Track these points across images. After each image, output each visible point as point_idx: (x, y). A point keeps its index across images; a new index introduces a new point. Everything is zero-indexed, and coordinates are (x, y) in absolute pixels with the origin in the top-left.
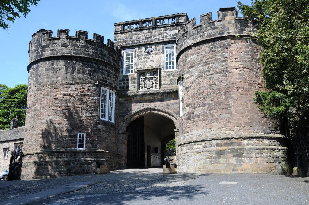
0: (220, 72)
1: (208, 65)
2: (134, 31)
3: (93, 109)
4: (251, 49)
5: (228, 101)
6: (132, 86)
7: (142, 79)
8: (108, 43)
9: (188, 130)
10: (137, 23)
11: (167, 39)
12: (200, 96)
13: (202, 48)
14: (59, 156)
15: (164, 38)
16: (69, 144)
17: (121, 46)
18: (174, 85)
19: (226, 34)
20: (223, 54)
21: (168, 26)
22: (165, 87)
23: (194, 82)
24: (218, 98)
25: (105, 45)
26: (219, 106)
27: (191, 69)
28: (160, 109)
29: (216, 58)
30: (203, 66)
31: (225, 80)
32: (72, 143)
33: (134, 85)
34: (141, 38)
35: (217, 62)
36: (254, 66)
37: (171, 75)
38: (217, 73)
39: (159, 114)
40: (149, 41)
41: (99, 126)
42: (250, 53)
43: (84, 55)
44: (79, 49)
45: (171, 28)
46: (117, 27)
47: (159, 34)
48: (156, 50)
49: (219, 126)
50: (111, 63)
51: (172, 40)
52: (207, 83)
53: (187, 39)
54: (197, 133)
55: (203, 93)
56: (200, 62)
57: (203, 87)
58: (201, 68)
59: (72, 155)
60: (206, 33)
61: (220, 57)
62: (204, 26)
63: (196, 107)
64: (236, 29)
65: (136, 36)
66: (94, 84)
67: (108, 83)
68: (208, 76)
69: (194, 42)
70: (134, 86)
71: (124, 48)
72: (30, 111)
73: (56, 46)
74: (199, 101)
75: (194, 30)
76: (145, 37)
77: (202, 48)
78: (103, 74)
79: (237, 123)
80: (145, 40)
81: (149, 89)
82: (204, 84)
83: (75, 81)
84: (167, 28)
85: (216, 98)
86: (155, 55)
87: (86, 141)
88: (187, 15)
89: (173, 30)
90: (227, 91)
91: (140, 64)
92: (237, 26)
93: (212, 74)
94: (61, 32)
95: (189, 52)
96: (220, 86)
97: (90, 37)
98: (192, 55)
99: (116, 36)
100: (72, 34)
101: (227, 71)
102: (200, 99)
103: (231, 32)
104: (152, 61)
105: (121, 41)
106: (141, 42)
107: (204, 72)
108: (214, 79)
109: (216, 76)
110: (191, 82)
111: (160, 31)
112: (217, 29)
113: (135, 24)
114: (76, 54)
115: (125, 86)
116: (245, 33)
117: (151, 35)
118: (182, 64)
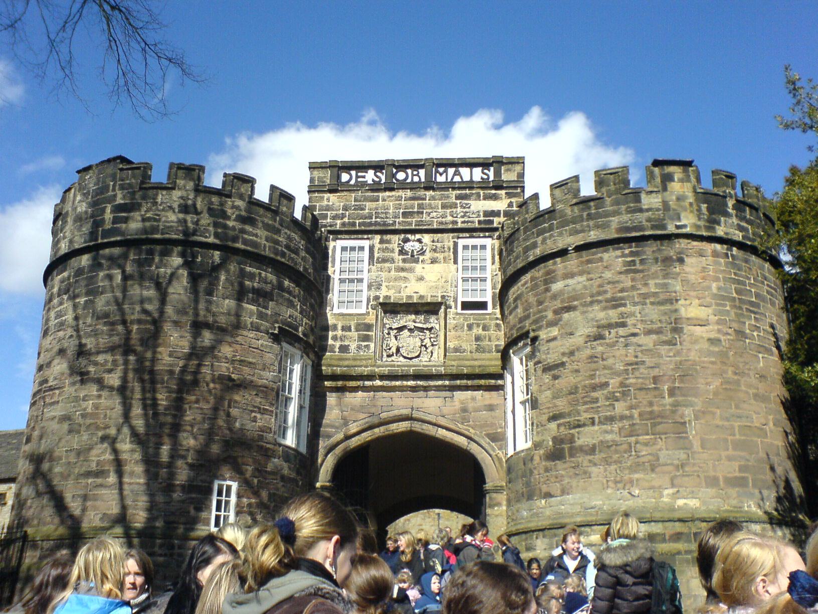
1: (622, 309)
3: (259, 408)
4: (735, 274)
5: (680, 412)
6: (359, 347)
7: (391, 328)
8: (304, 216)
9: (555, 488)
10: (378, 167)
11: (468, 222)
12: (594, 395)
13: (601, 259)
16: (189, 512)
17: (329, 228)
18: (487, 355)
19: (671, 229)
20: (666, 281)
21: (470, 185)
23: (576, 353)
24: (651, 404)
25: (295, 221)
26: (654, 425)
27: (566, 316)
28: (442, 421)
29: (644, 290)
30: (605, 308)
31: (671, 354)
33: (366, 343)
35: (648, 301)
36: (745, 323)
38: (649, 332)
39: (437, 436)
40: (413, 222)
42: (733, 286)
45: (478, 195)
46: (316, 173)
48: (435, 251)
49: (656, 483)
51: (483, 226)
52: (619, 357)
53: (551, 229)
54: (585, 500)
55: (606, 384)
56: (595, 298)
57: (605, 368)
58: (599, 314)
60: (615, 221)
61: (657, 290)
62: (608, 200)
63: (584, 425)
64: (699, 219)
65: (373, 205)
66: (267, 333)
68: (622, 339)
69: (579, 240)
70: (367, 347)
71: (337, 233)
72: (55, 399)
74: (592, 408)
75: (576, 208)
76: (401, 211)
77: (601, 259)
78: (291, 305)
79: (705, 477)
80: (401, 219)
81: (411, 359)
82: (610, 361)
84: (468, 191)
85: (645, 402)
86: (432, 263)
87: (238, 505)
89: (484, 199)
90: (677, 385)
91: (384, 284)
92: (699, 210)
93: (634, 335)
96: (657, 370)
98: (570, 275)
101: (677, 330)
103: (685, 226)
104: (421, 279)
105: (329, 213)
107: (610, 326)
108: (640, 348)
109: (648, 341)
110: (567, 351)
111: (448, 197)
112: (647, 214)
116: (720, 231)
118: (532, 299)
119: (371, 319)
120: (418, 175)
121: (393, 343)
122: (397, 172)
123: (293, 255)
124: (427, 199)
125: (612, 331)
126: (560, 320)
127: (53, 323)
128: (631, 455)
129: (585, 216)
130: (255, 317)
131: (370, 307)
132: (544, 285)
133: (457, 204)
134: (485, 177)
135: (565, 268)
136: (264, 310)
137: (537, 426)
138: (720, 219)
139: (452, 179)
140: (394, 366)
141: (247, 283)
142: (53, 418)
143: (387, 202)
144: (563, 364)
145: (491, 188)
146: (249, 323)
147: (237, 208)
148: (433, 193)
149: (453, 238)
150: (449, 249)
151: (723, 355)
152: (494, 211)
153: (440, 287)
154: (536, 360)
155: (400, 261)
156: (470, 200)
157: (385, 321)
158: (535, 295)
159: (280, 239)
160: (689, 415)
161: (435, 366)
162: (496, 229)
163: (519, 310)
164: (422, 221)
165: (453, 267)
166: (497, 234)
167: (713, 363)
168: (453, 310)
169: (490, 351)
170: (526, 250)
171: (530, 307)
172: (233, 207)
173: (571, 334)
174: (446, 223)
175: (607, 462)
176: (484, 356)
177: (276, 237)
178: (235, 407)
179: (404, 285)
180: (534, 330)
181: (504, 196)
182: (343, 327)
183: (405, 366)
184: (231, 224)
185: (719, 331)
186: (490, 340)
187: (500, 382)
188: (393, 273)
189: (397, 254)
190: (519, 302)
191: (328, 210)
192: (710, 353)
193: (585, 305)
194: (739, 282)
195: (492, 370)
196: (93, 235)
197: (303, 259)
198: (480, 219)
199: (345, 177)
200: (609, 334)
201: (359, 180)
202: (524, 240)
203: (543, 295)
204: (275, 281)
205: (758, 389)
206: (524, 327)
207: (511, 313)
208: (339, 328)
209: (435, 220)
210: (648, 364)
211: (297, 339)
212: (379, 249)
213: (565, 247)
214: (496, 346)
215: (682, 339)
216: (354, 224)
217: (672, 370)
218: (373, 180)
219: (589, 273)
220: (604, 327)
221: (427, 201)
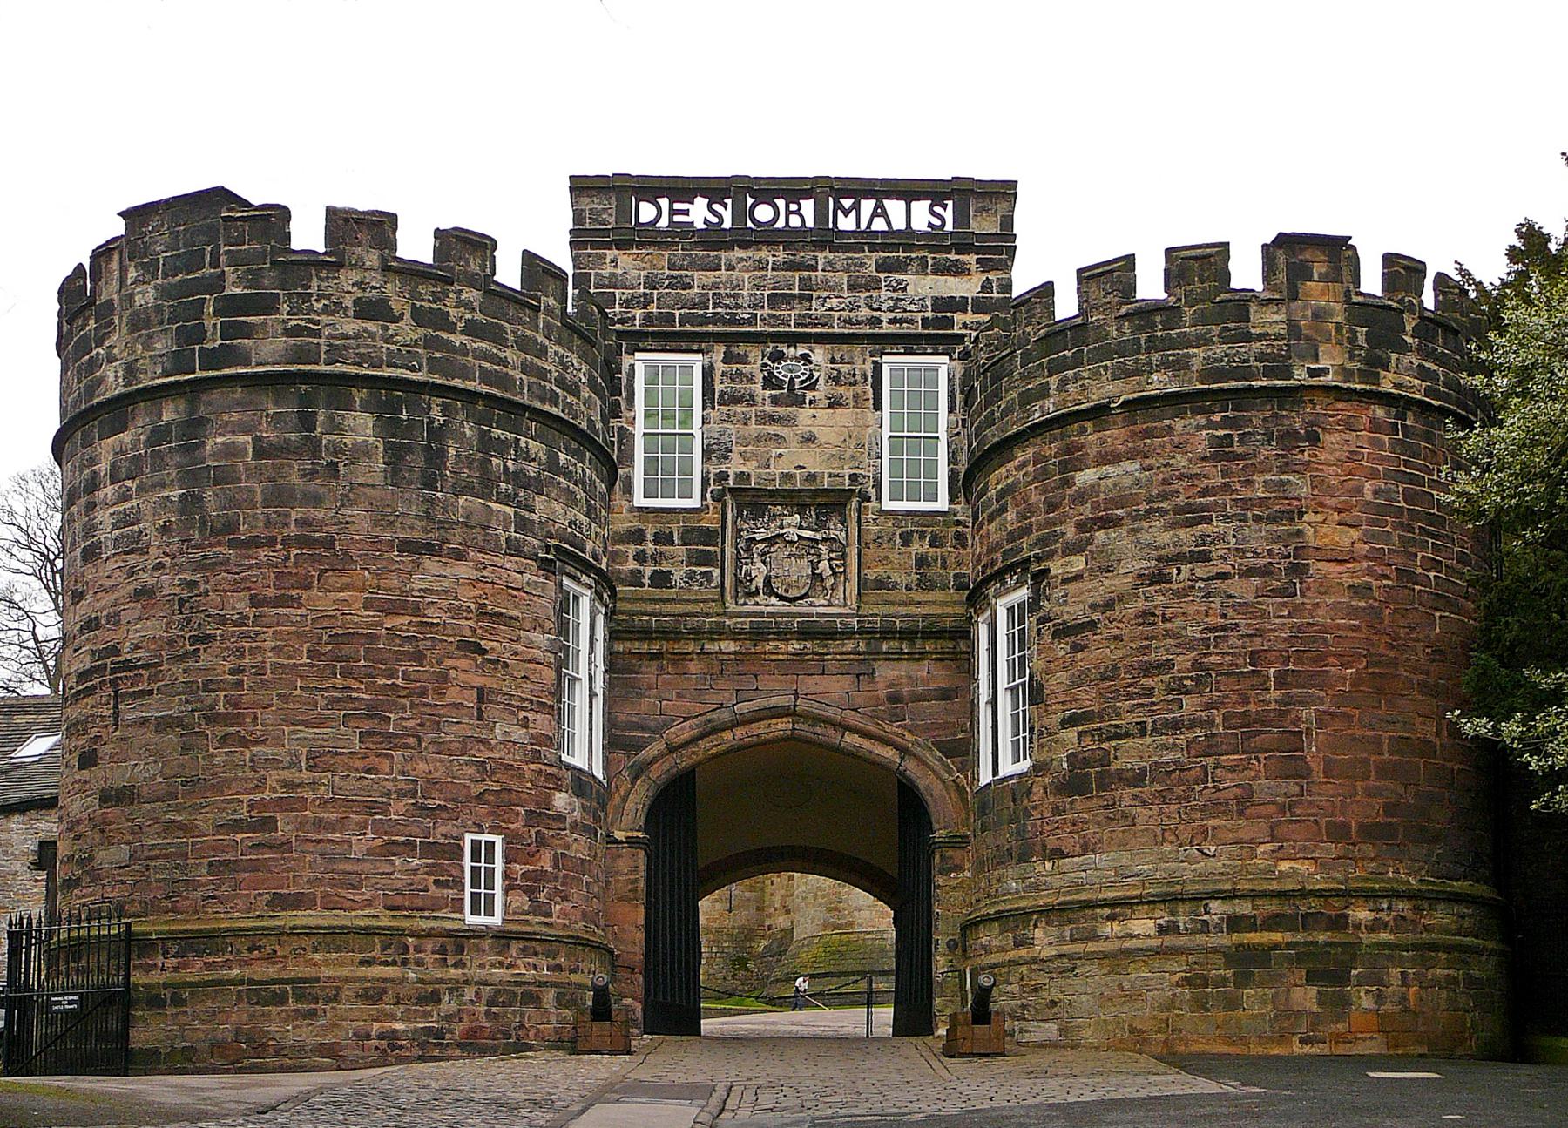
0: (1265, 572)
3: (531, 702)
6: (690, 576)
10: (715, 189)
11: (901, 321)
12: (1148, 682)
14: (376, 953)
15: (885, 317)
17: (618, 327)
18: (938, 596)
21: (905, 240)
24: (1245, 700)
26: (1247, 737)
27: (1100, 536)
30: (1173, 526)
31: (1286, 613)
32: (436, 883)
33: (703, 569)
34: (745, 293)
37: (922, 536)
38: (1248, 573)
41: (558, 795)
43: (483, 381)
45: (923, 262)
46: (586, 204)
47: (851, 288)
48: (836, 380)
55: (1169, 664)
58: (1159, 534)
59: (443, 951)
63: (1127, 735)
65: (706, 278)
66: (536, 558)
68: (1200, 584)
69: (1124, 391)
70: (707, 576)
71: (637, 341)
72: (144, 686)
73: (326, 311)
74: (1142, 705)
76: (767, 292)
78: (571, 500)
80: (767, 310)
85: (1235, 698)
86: (830, 406)
89: (935, 272)
94: (340, 222)
95: (1092, 439)
96: (1259, 640)
97: (415, 245)
100: (415, 245)
101: (1298, 570)
102: (1150, 696)
104: (810, 439)
106: (746, 316)
107: (1179, 559)
109: (1243, 589)
111: (862, 265)
113: (701, 203)
114: (446, 376)
115: (648, 570)
117: (806, 283)
118: (1036, 498)
119: (710, 522)
120: (798, 212)
121: (758, 570)
122: (754, 206)
124: (820, 268)
125: (1183, 567)
126: (1090, 542)
127: (107, 533)
128: (1205, 788)
131: (708, 495)
134: (937, 222)
135: (1102, 442)
137: (1041, 733)
138: (1389, 358)
140: (761, 615)
142: (144, 722)
143: (736, 273)
144: (1092, 625)
147: (467, 305)
148: (831, 256)
151: (1374, 614)
154: (1042, 613)
155: (768, 401)
158: (1044, 491)
160: (1308, 720)
161: (839, 616)
162: (960, 338)
163: (1010, 516)
164: (810, 316)
165: (871, 415)
167: (1354, 628)
169: (945, 588)
170: (1027, 399)
172: (460, 304)
174: (859, 323)
175: (1163, 798)
176: (931, 596)
178: (490, 701)
179: (775, 452)
180: (1039, 559)
181: (974, 267)
182: (656, 534)
183: (782, 615)
184: (457, 339)
185: (1370, 572)
187: (962, 646)
188: (753, 425)
189: (760, 386)
192: (1353, 612)
194: (1412, 479)
195: (948, 623)
196: (180, 362)
198: (926, 315)
200: (1178, 574)
201: (677, 218)
202: (1023, 378)
205: (1427, 674)
206: (1019, 550)
207: (991, 519)
208: (650, 537)
210: (1244, 630)
214: (956, 576)
215: (1304, 585)
216: (670, 319)
217: (1285, 640)
218: (706, 221)
220: (1169, 560)
221: (819, 273)
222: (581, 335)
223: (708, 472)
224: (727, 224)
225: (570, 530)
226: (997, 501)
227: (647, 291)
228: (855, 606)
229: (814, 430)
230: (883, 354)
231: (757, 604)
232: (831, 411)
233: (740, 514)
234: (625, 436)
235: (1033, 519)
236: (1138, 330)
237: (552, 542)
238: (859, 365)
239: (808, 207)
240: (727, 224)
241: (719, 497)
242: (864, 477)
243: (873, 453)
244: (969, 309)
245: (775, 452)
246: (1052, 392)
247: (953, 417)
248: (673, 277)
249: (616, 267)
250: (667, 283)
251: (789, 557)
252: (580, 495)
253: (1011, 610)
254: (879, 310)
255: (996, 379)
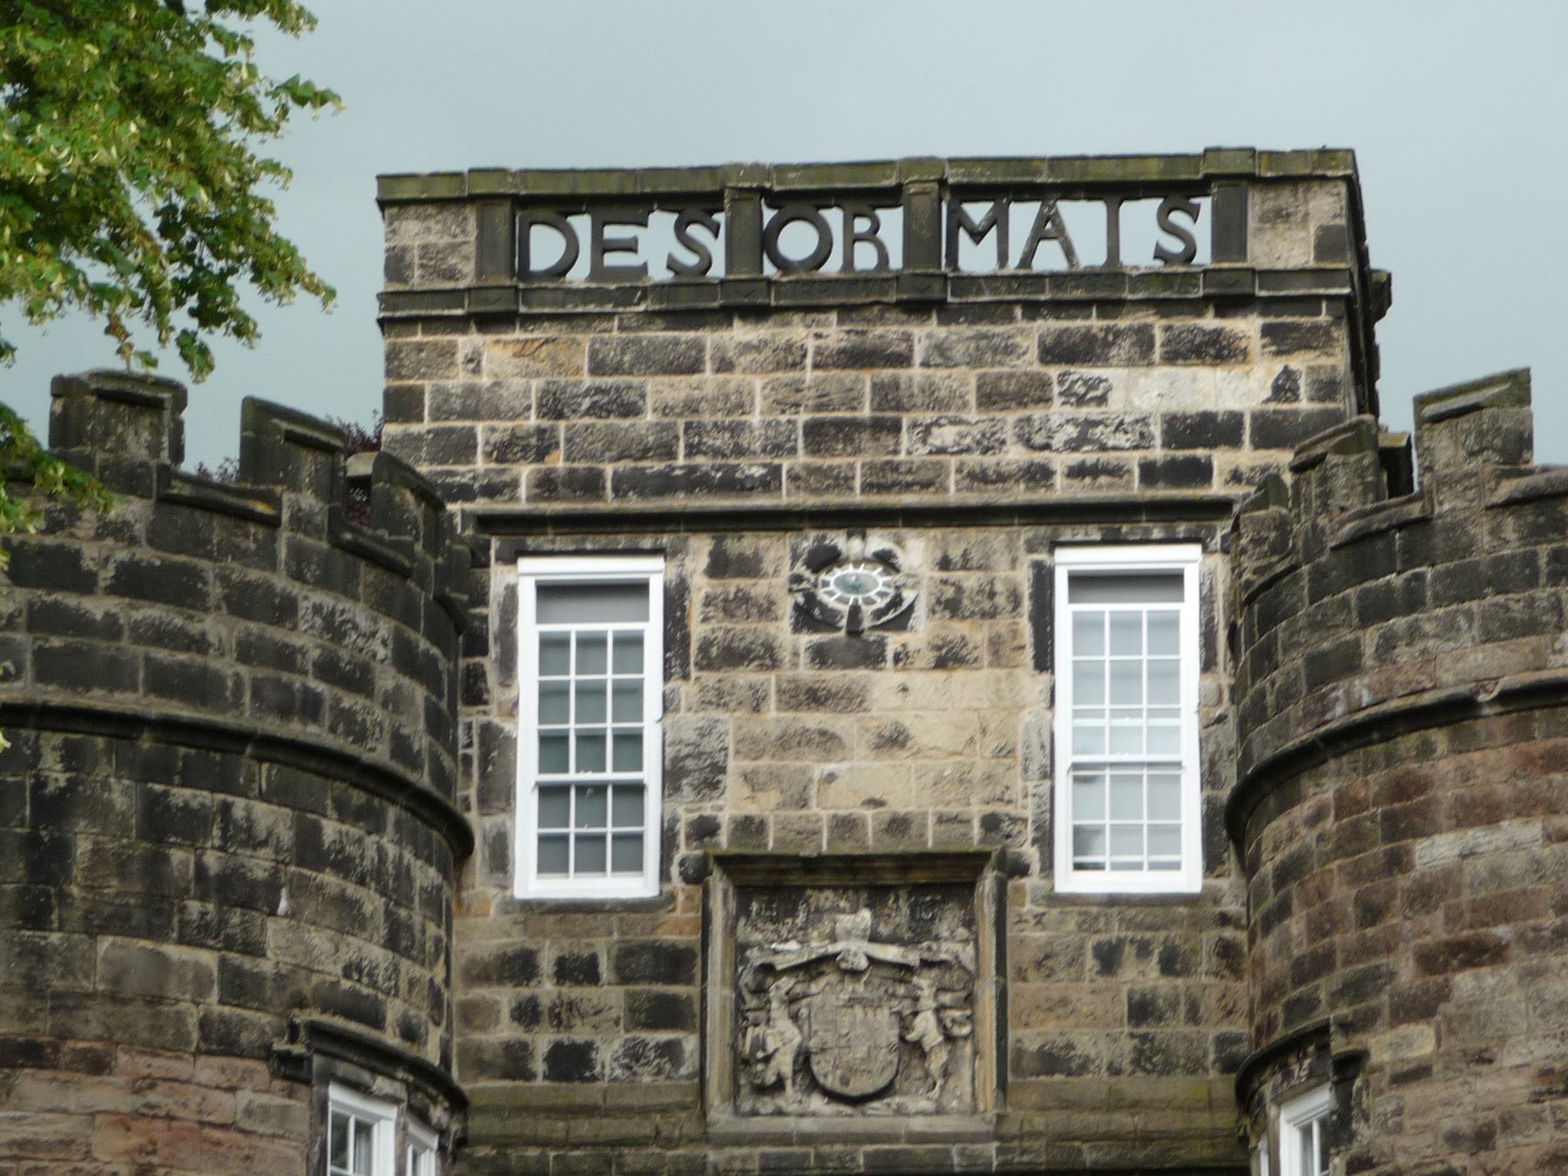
2: (650, 316)
6: (634, 1054)
7: (768, 969)
11: (1093, 471)
15: (1060, 462)
17: (481, 505)
18: (1177, 1086)
22: (1067, 1105)
23: (1500, 1141)
27: (1464, 982)
33: (663, 1036)
37: (1144, 950)
44: (99, 616)
45: (1144, 340)
46: (415, 232)
48: (951, 606)
50: (413, 761)
51: (1162, 492)
53: (1412, 601)
66: (266, 1053)
67: (391, 1038)
70: (670, 1051)
76: (803, 417)
78: (349, 916)
80: (802, 458)
81: (858, 1101)
83: (61, 1017)
84: (1095, 323)
86: (941, 664)
88: (1353, 186)
89: (1172, 357)
91: (733, 764)
99: (409, 360)
104: (894, 740)
105: (480, 428)
106: (757, 472)
110: (1465, 1126)
111: (1009, 350)
115: (543, 1041)
117: (887, 396)
118: (1342, 893)
119: (675, 931)
120: (872, 236)
122: (778, 225)
123: (349, 701)
124: (918, 358)
126: (1443, 994)
129: (1543, 561)
130: (214, 997)
131: (675, 870)
132: (1388, 838)
133: (1045, 384)
135: (1466, 776)
136: (247, 963)
139: (1027, 260)
140: (784, 1139)
141: (178, 856)
143: (735, 378)
145: (1196, 307)
146: (192, 1022)
148: (941, 332)
149: (1031, 549)
150: (1015, 599)
152: (1207, 418)
153: (977, 774)
154: (1355, 1149)
155: (804, 658)
156: (1105, 361)
157: (744, 932)
158: (1355, 877)
159: (297, 640)
161: (957, 1138)
162: (1220, 507)
163: (1296, 925)
164: (895, 468)
165: (1030, 683)
166: (1223, 528)
168: (1032, 882)
169: (1195, 1066)
171: (1335, 925)
173: (1483, 1059)
174: (1002, 478)
177: (277, 634)
180: (1347, 1027)
183: (831, 1139)
186: (1193, 1016)
189: (786, 623)
190: (1293, 887)
191: (475, 415)
193: (1533, 943)
197: (393, 701)
199: (545, 246)
201: (611, 259)
203: (1381, 882)
204: (286, 835)
206: (1306, 1005)
207: (1268, 924)
208: (546, 963)
209: (953, 462)
211: (383, 1059)
212: (709, 601)
213: (1463, 689)
214: (1223, 1041)
218: (672, 264)
219: (1552, 809)
221: (916, 373)
222: (374, 559)
223: (674, 820)
224: (718, 271)
225: (346, 984)
226: (1277, 887)
227: (546, 423)
228: (991, 1114)
229: (908, 721)
230: (1054, 545)
231: (779, 1113)
232: (940, 675)
233: (743, 909)
234: (495, 744)
235: (1337, 938)
236: (1534, 534)
237: (301, 1017)
238: (1002, 572)
239: (892, 221)
240: (718, 271)
241: (697, 875)
242: (1014, 820)
243: (1034, 767)
244: (1247, 436)
245: (819, 769)
246: (1368, 660)
247: (1210, 682)
248: (599, 390)
249: (476, 371)
250: (586, 403)
251: (851, 1002)
252: (372, 902)
253: (1306, 1132)
254: (1047, 447)
255: (1269, 620)
